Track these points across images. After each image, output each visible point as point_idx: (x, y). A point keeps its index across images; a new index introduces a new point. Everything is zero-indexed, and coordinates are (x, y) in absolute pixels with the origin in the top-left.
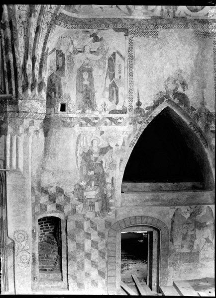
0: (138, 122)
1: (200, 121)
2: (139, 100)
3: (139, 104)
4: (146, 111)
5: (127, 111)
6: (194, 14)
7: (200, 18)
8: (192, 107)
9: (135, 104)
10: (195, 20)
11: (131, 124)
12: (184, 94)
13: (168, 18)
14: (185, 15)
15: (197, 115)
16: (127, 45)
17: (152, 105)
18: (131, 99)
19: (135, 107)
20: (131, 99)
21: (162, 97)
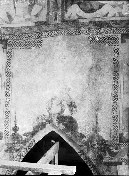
0: (15, 150)
1: (90, 151)
2: (16, 125)
3: (16, 129)
4: (24, 138)
5: (2, 137)
6: (89, 15)
7: (97, 20)
8: (81, 134)
9: (12, 129)
10: (90, 22)
11: (6, 151)
12: (71, 118)
13: (55, 22)
14: (76, 17)
15: (87, 143)
16: (5, 60)
17: (31, 131)
18: (7, 123)
19: (11, 132)
20: (7, 123)
21: (44, 121)
